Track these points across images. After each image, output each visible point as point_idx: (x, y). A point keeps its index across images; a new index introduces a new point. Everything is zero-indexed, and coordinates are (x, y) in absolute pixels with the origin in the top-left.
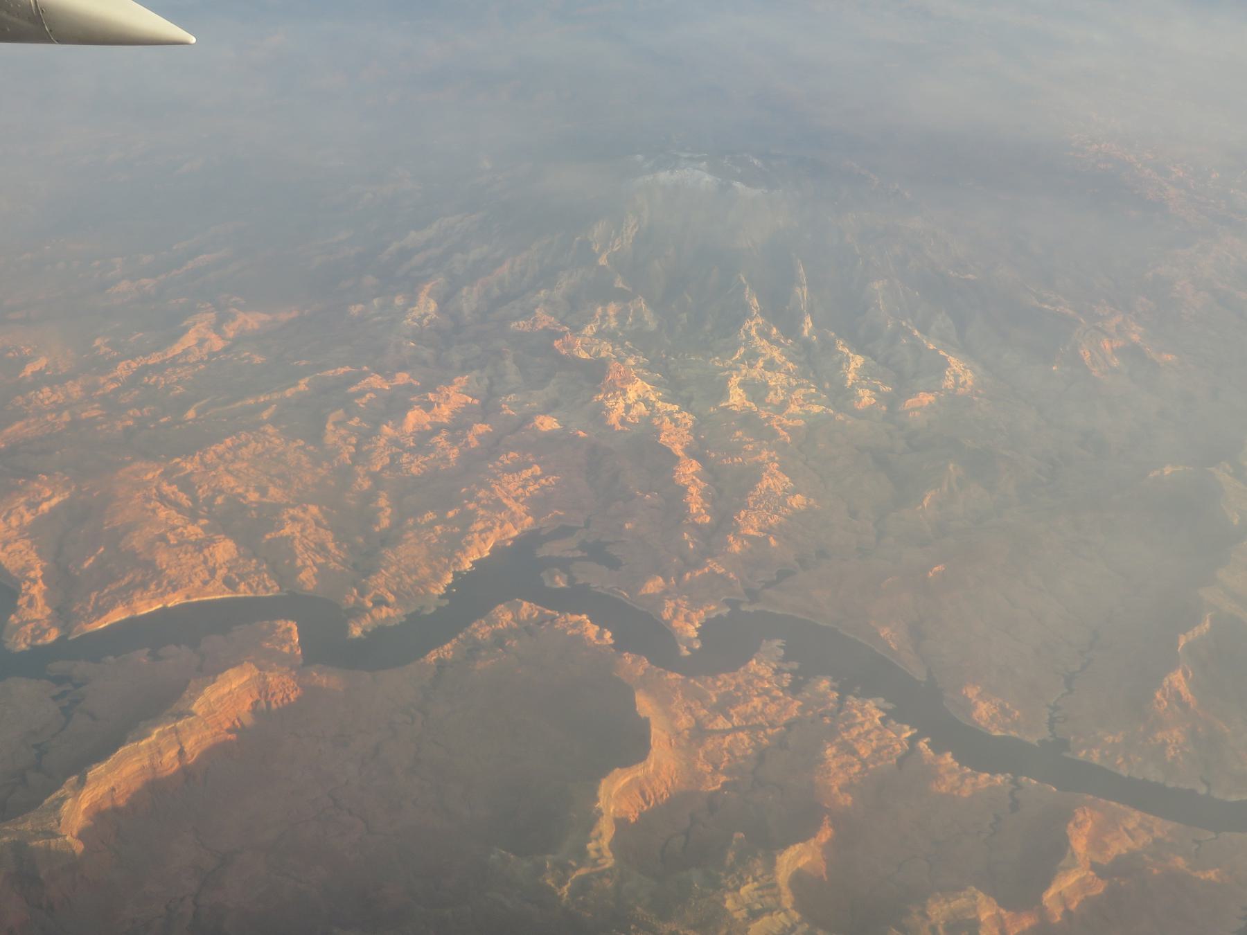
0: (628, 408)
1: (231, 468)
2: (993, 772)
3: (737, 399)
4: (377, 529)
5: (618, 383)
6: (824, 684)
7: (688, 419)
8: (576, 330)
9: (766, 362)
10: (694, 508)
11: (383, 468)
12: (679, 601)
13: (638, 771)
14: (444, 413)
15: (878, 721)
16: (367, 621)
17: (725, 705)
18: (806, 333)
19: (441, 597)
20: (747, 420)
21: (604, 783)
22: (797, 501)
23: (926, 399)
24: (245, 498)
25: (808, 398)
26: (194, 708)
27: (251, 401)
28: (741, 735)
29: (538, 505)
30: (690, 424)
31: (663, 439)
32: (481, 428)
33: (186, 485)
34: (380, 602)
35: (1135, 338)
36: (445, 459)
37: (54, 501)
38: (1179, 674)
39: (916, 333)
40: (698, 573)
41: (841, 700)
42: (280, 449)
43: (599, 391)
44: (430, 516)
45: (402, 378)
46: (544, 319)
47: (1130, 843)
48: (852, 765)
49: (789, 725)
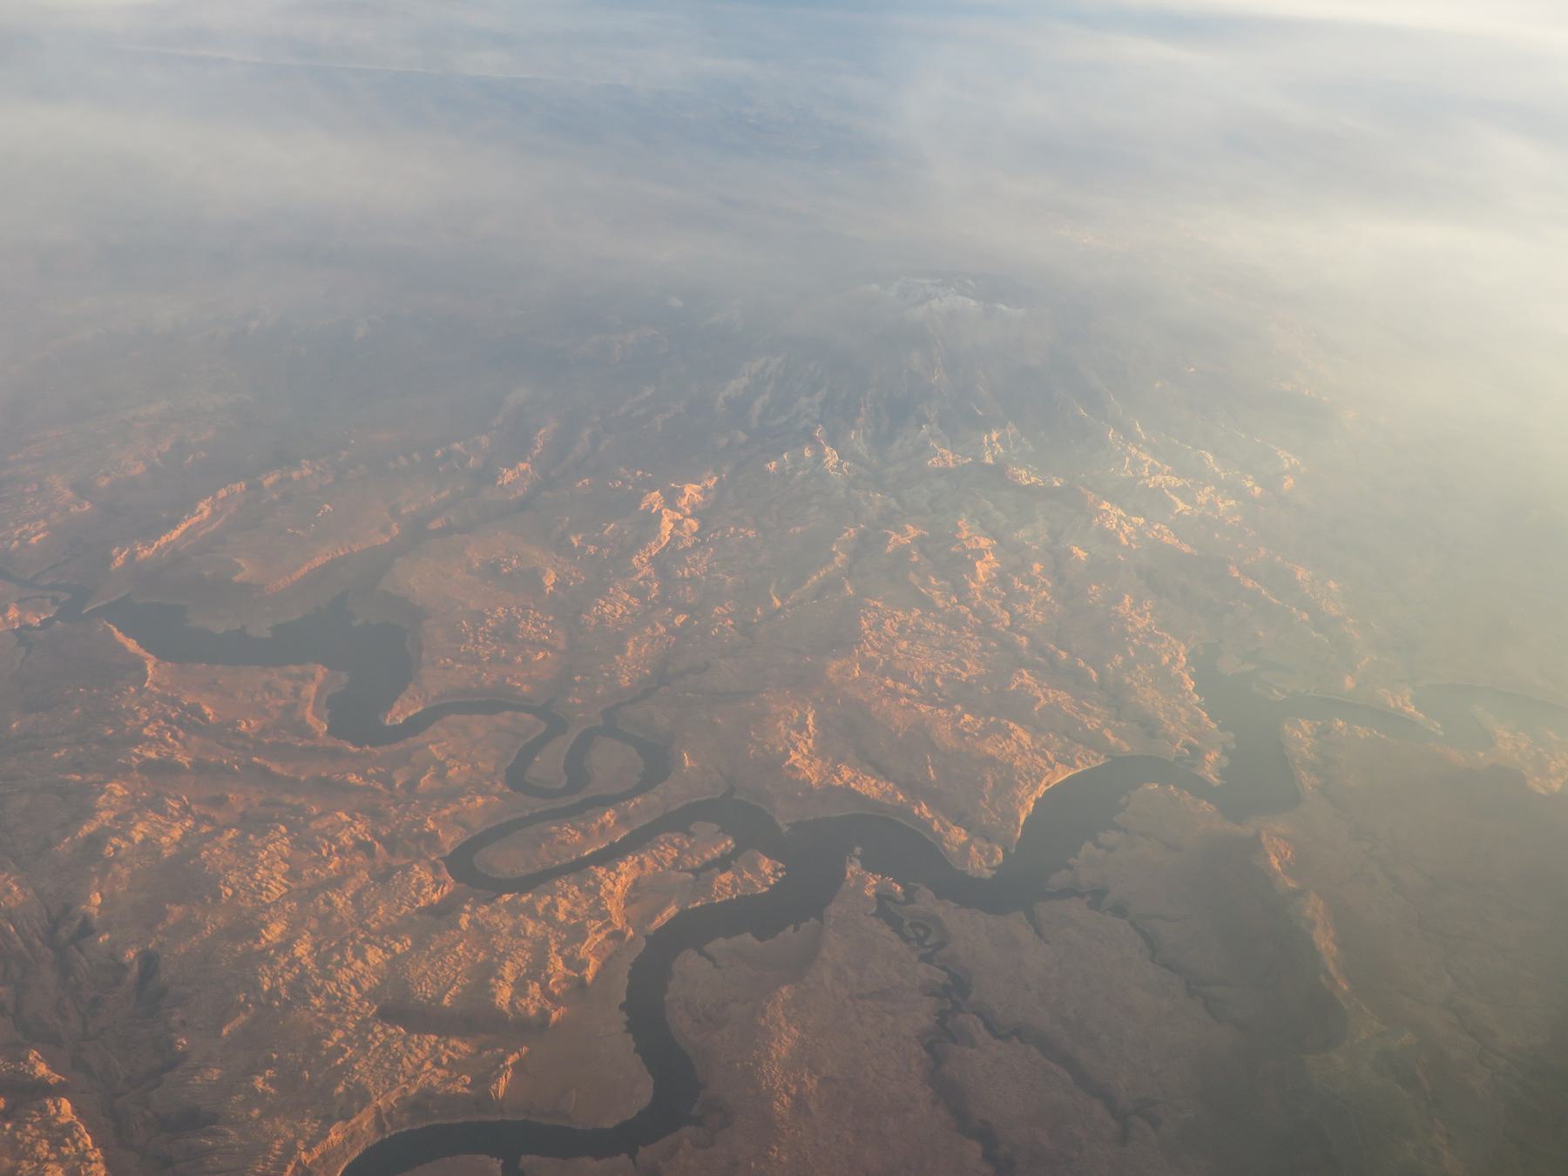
37: (810, 718)
44: (1119, 659)
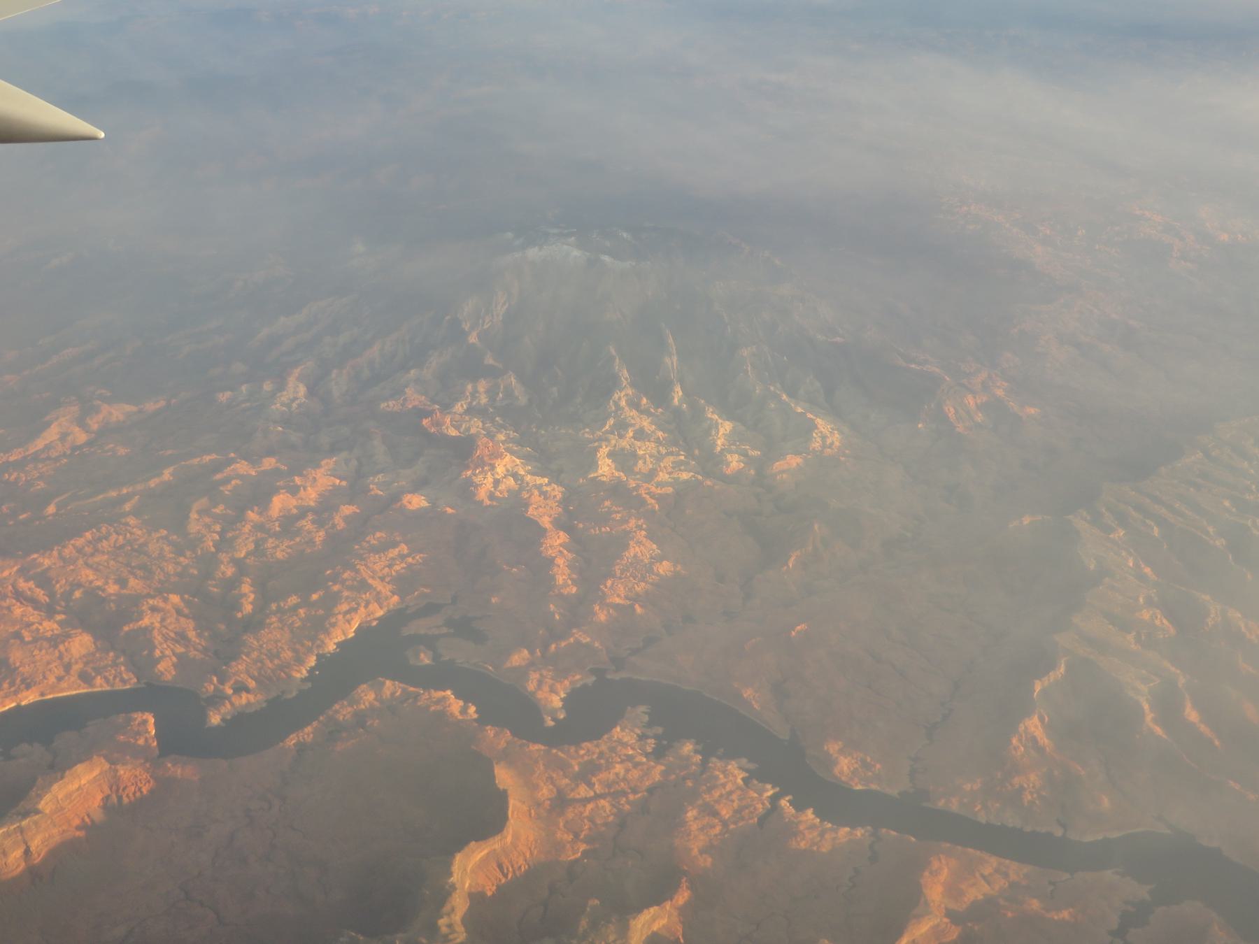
0: (497, 483)
1: (90, 561)
2: (853, 827)
3: (606, 469)
4: (239, 615)
5: (486, 459)
6: (688, 748)
7: (557, 491)
8: (446, 407)
9: (636, 432)
10: (560, 580)
11: (248, 554)
12: (544, 673)
13: (495, 844)
14: (311, 496)
15: (740, 781)
16: (227, 708)
17: (587, 773)
18: (676, 402)
19: (304, 680)
20: (616, 490)
21: (458, 857)
22: (664, 568)
23: (794, 461)
24: (103, 590)
25: (677, 465)
26: (40, 807)
27: (114, 494)
28: (602, 802)
29: (403, 584)
30: (559, 496)
31: (531, 512)
32: (348, 510)
33: (44, 580)
34: (240, 688)
35: (1000, 393)
36: (311, 542)
38: (1036, 719)
39: (784, 397)
40: (563, 644)
41: (704, 763)
42: (142, 540)
43: (467, 468)
45: (269, 463)
46: (414, 398)
47: (986, 888)
48: (713, 827)
49: (651, 791)
